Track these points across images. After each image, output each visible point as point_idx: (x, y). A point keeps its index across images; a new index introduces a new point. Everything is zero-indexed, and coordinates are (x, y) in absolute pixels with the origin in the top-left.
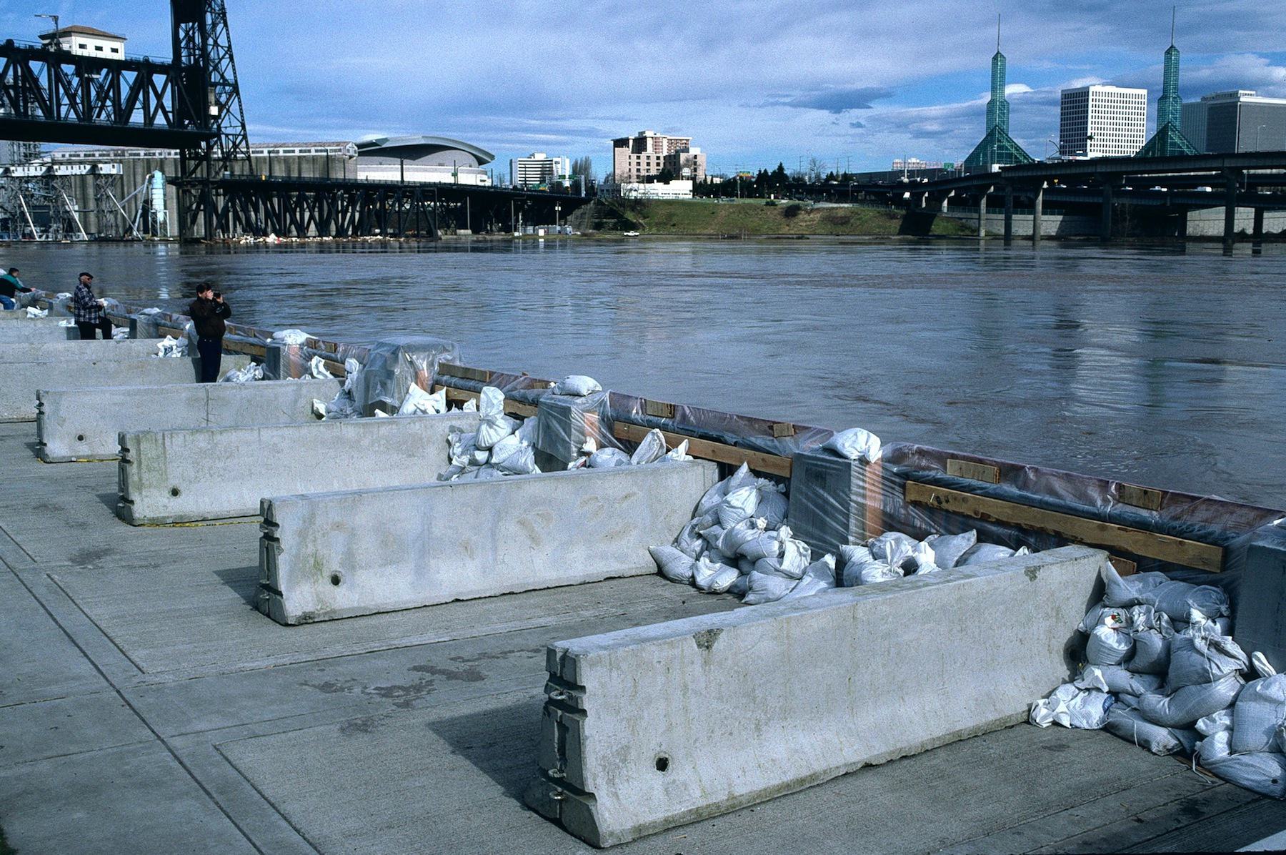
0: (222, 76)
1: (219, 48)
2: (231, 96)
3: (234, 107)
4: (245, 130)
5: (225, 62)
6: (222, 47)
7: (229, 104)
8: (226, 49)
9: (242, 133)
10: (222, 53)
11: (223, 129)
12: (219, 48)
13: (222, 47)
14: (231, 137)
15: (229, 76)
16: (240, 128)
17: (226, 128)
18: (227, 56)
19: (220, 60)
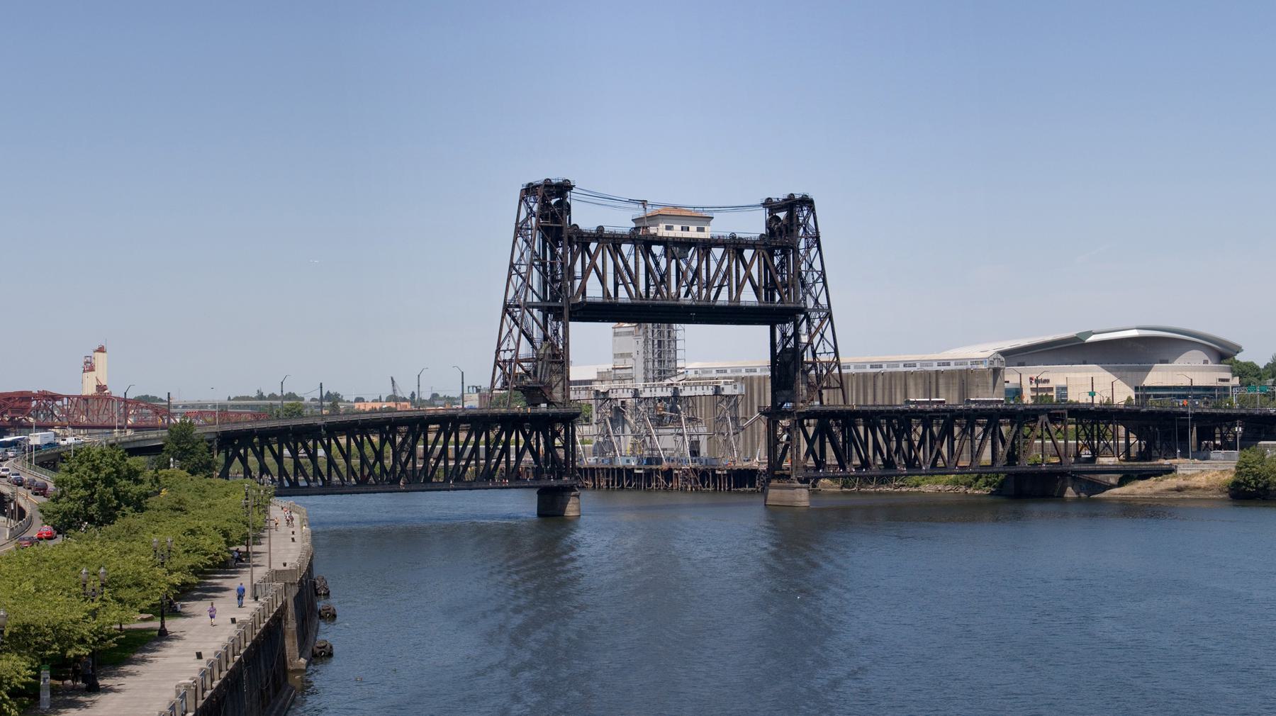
0: (816, 301)
1: (814, 273)
2: (822, 322)
3: (828, 335)
4: (838, 359)
5: (819, 286)
6: (817, 272)
7: (824, 327)
8: (820, 273)
9: (836, 359)
10: (816, 276)
11: (818, 355)
12: (814, 273)
13: (817, 272)
14: (825, 364)
15: (823, 300)
16: (834, 354)
17: (820, 354)
18: (821, 280)
19: (815, 282)
